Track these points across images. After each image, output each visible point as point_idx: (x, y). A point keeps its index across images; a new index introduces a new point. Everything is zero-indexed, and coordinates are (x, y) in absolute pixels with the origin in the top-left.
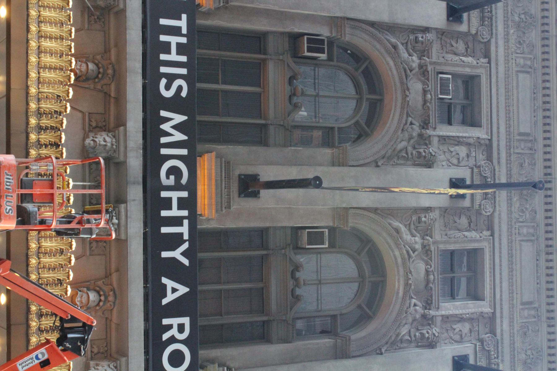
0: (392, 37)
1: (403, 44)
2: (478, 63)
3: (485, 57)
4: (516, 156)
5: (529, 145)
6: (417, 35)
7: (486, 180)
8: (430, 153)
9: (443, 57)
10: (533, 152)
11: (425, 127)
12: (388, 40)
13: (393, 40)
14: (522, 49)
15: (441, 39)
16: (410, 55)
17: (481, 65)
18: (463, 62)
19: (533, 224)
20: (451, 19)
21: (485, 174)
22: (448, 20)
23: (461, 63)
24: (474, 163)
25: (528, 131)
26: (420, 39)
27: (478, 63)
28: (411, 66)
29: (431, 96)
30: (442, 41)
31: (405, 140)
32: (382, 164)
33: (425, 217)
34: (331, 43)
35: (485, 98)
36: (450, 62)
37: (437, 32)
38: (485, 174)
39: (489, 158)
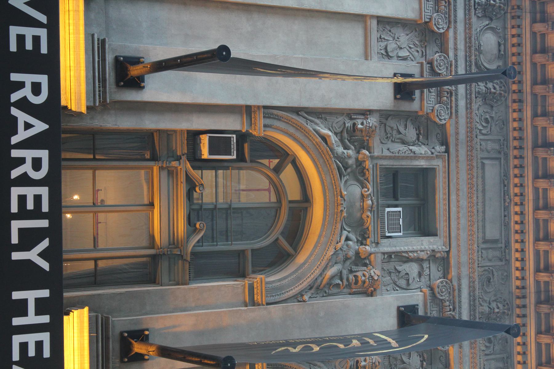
0: (321, 125)
1: (336, 134)
2: (432, 153)
3: (442, 145)
4: (481, 270)
5: (497, 253)
6: (354, 121)
7: (442, 303)
8: (372, 277)
9: (388, 149)
10: (503, 263)
11: (364, 242)
12: (317, 132)
13: (325, 131)
14: (489, 129)
15: (385, 125)
16: (345, 148)
17: (437, 155)
18: (414, 153)
19: (502, 356)
20: (398, 96)
21: (442, 296)
22: (395, 98)
23: (412, 155)
24: (429, 282)
25: (497, 237)
26: (360, 126)
27: (432, 153)
28: (347, 163)
29: (372, 201)
30: (387, 127)
31: (339, 263)
32: (310, 297)
33: (365, 360)
34: (242, 137)
35: (441, 191)
36: (397, 154)
37: (381, 116)
38: (442, 296)
39: (446, 273)
